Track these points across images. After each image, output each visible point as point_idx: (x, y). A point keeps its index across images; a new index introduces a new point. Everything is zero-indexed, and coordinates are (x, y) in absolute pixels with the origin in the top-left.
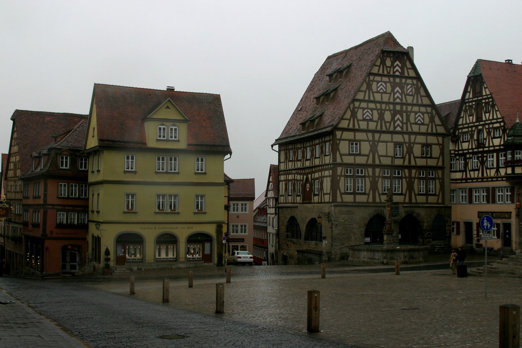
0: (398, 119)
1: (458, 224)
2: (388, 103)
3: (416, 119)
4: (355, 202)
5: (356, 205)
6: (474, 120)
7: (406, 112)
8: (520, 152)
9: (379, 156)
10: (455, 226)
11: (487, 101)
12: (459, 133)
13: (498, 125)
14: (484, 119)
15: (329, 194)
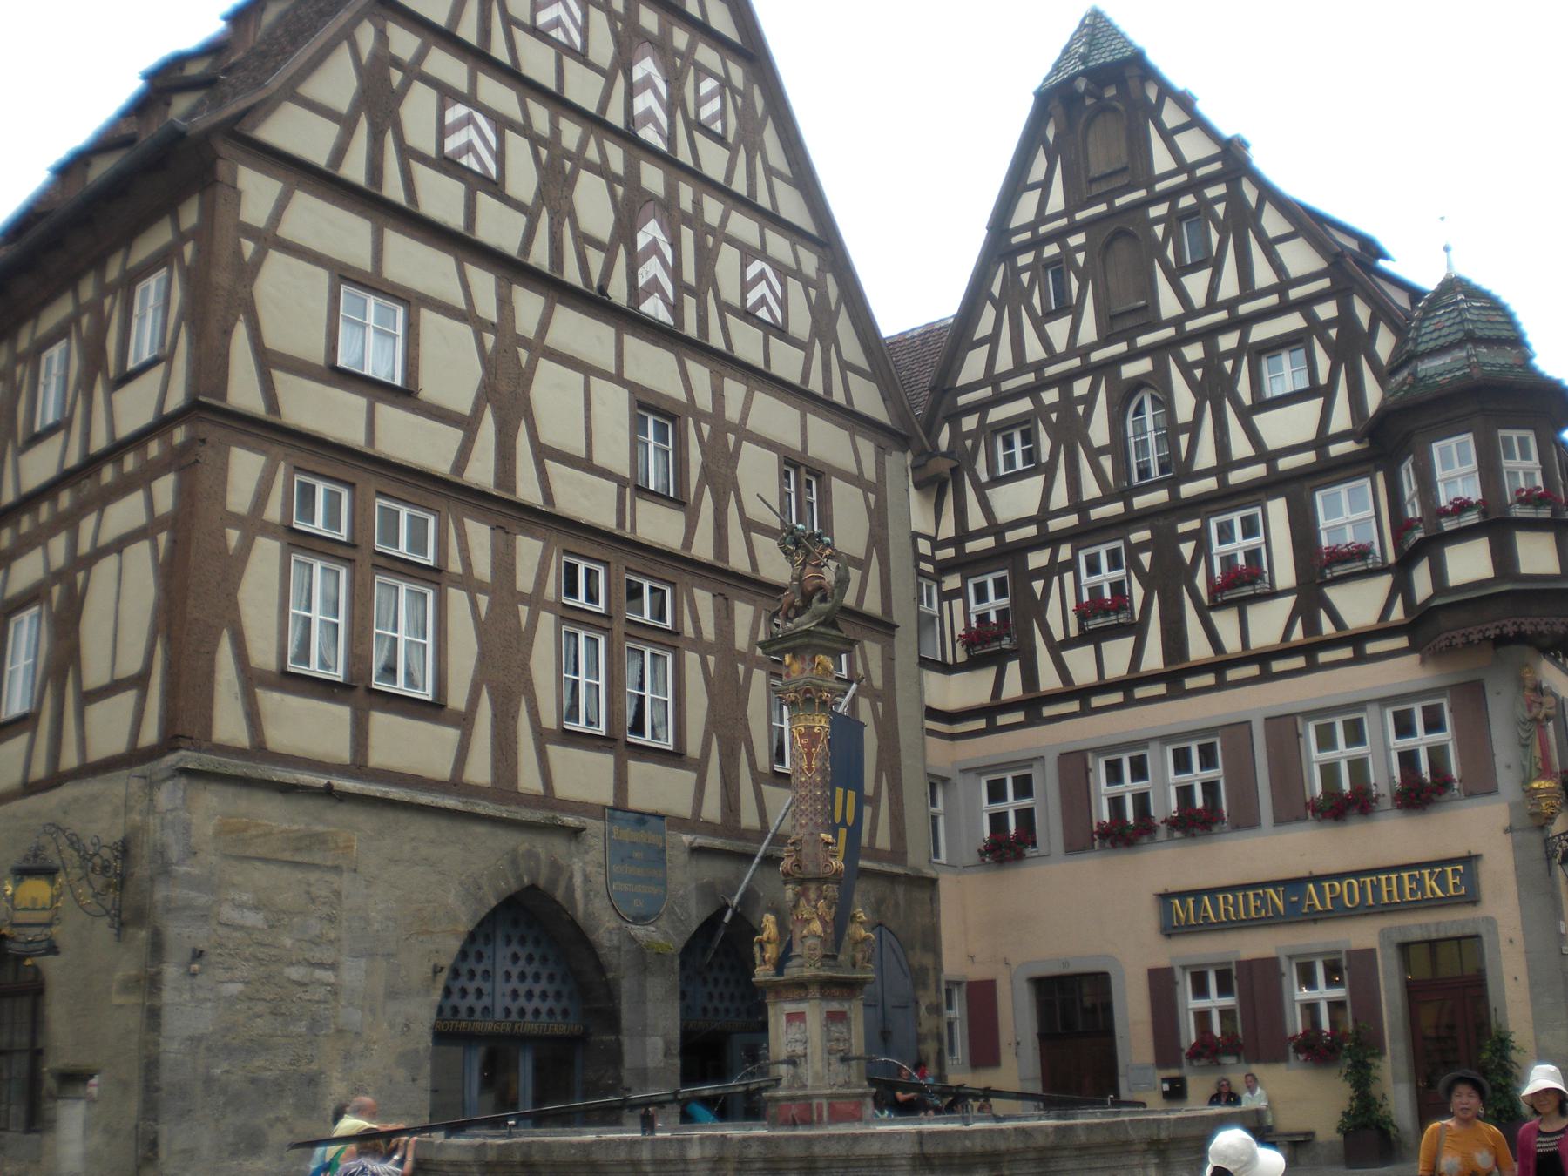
0: (653, 248)
1: (982, 995)
2: (595, 122)
3: (746, 287)
4: (358, 767)
5: (357, 790)
6: (1088, 331)
7: (695, 220)
8: (1523, 442)
9: (542, 452)
10: (958, 1012)
11: (1187, 201)
12: (956, 434)
13: (1293, 322)
14: (1169, 306)
15: (139, 681)
